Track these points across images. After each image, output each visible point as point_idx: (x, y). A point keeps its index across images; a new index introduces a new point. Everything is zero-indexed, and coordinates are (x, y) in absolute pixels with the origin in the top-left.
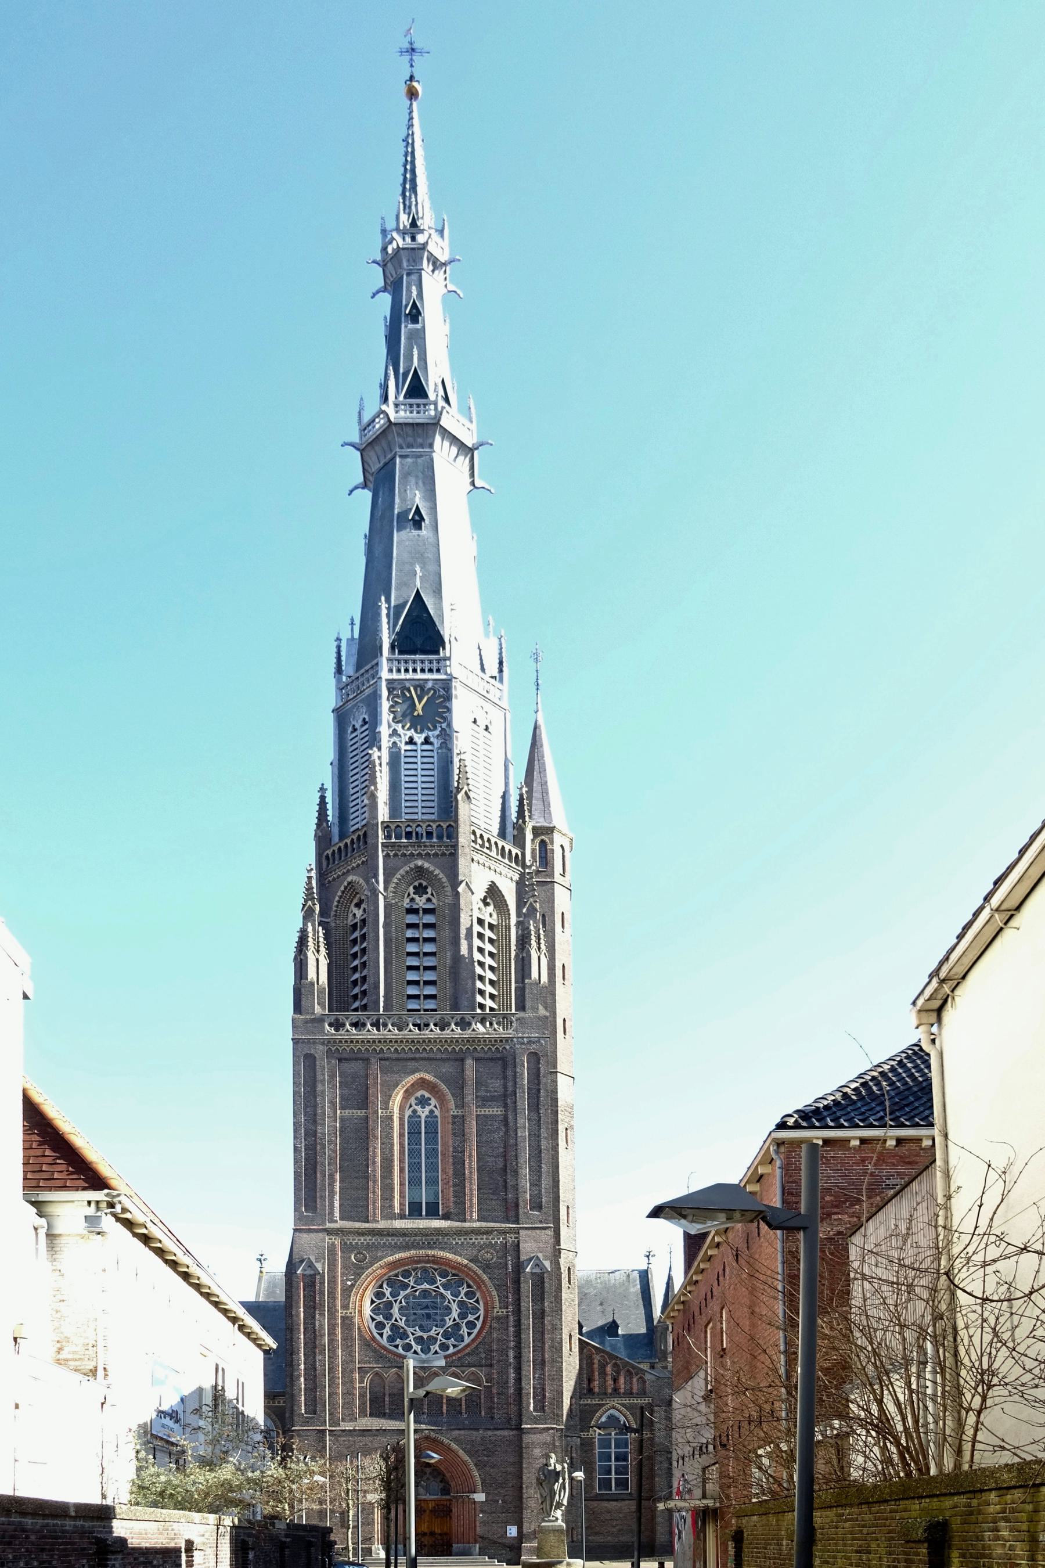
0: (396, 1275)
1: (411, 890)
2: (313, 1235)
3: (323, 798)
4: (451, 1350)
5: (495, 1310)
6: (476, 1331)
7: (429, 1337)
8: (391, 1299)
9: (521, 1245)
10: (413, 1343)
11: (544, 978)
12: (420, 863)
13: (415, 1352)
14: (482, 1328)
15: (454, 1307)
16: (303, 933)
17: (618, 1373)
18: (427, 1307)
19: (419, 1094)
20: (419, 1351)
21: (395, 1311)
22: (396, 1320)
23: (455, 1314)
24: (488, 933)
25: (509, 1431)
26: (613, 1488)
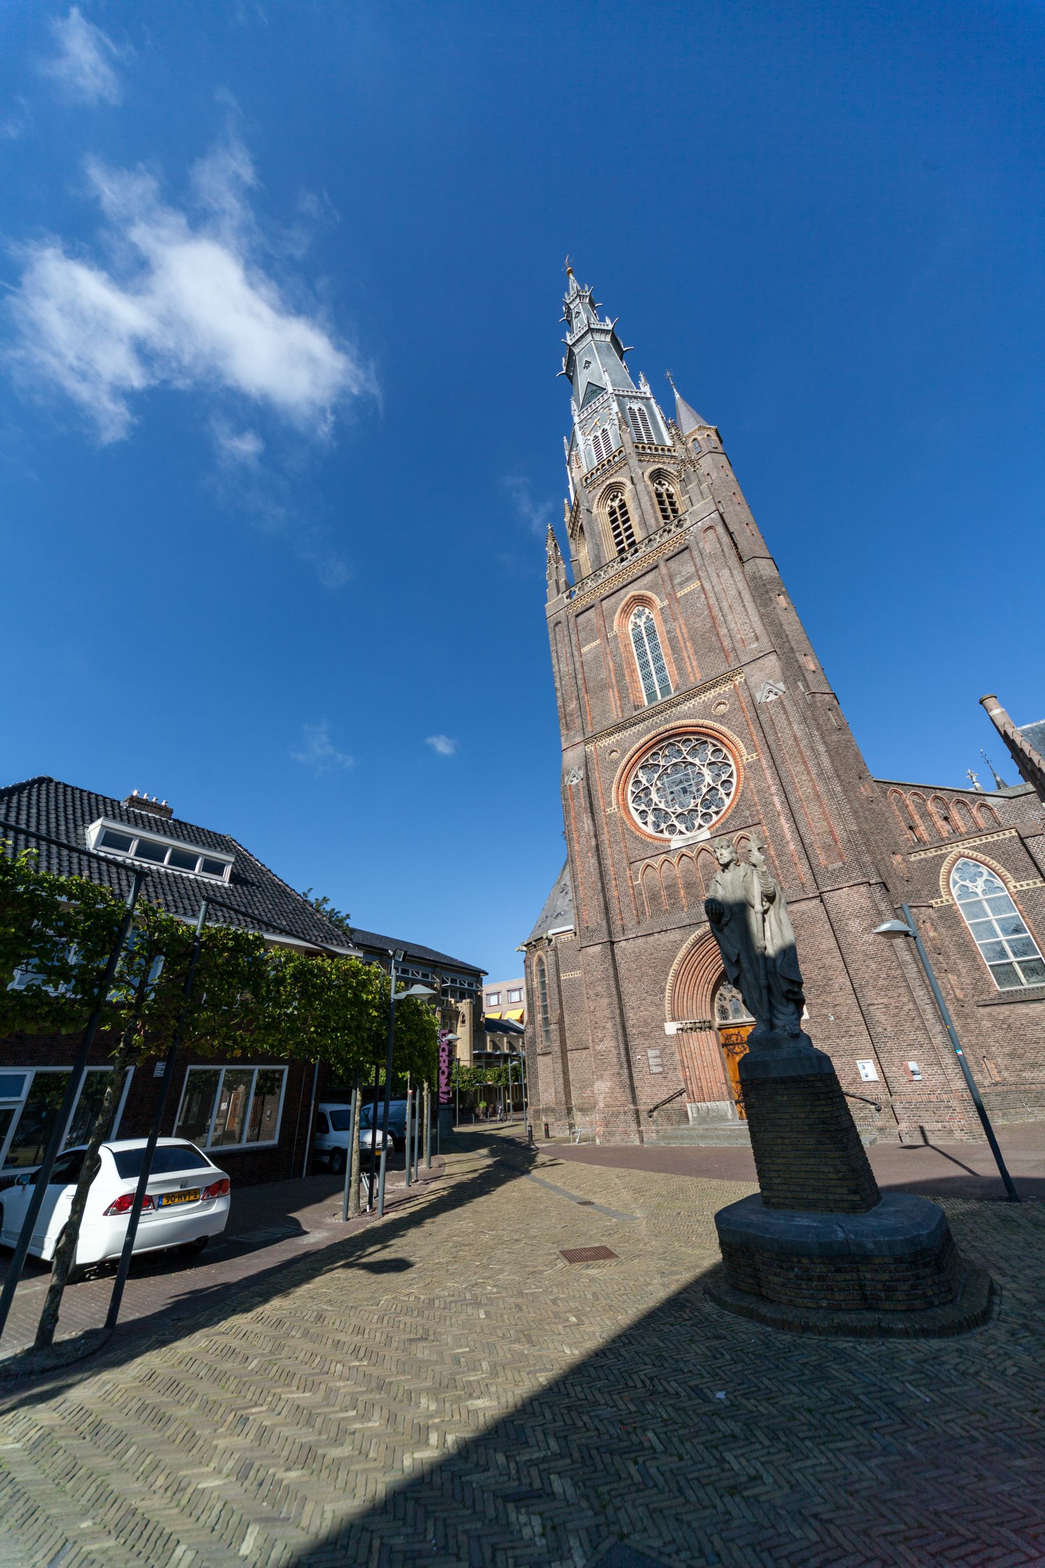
0: (647, 760)
1: (609, 502)
4: (715, 818)
5: (744, 758)
6: (733, 790)
8: (647, 785)
10: (676, 823)
12: (608, 482)
13: (681, 833)
14: (738, 783)
15: (705, 771)
17: (947, 809)
18: (681, 782)
19: (635, 611)
20: (683, 829)
21: (654, 796)
22: (656, 804)
23: (708, 779)
25: (807, 902)
26: (1023, 980)
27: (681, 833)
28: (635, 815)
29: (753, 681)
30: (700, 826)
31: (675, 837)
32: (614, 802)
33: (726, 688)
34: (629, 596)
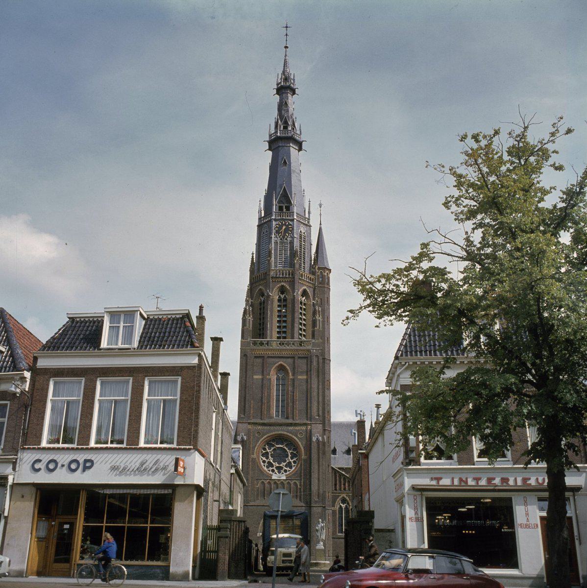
2: (244, 425)
3: (253, 256)
4: (288, 473)
7: (280, 467)
9: (312, 430)
11: (321, 329)
12: (282, 284)
13: (276, 473)
16: (245, 309)
24: (303, 312)
27: (276, 473)
28: (261, 461)
29: (313, 431)
30: (283, 473)
31: (274, 474)
32: (255, 454)
33: (304, 428)
34: (280, 363)
